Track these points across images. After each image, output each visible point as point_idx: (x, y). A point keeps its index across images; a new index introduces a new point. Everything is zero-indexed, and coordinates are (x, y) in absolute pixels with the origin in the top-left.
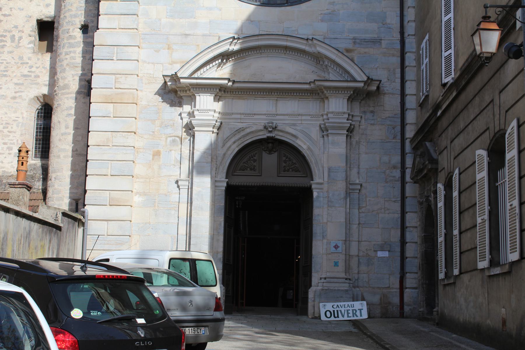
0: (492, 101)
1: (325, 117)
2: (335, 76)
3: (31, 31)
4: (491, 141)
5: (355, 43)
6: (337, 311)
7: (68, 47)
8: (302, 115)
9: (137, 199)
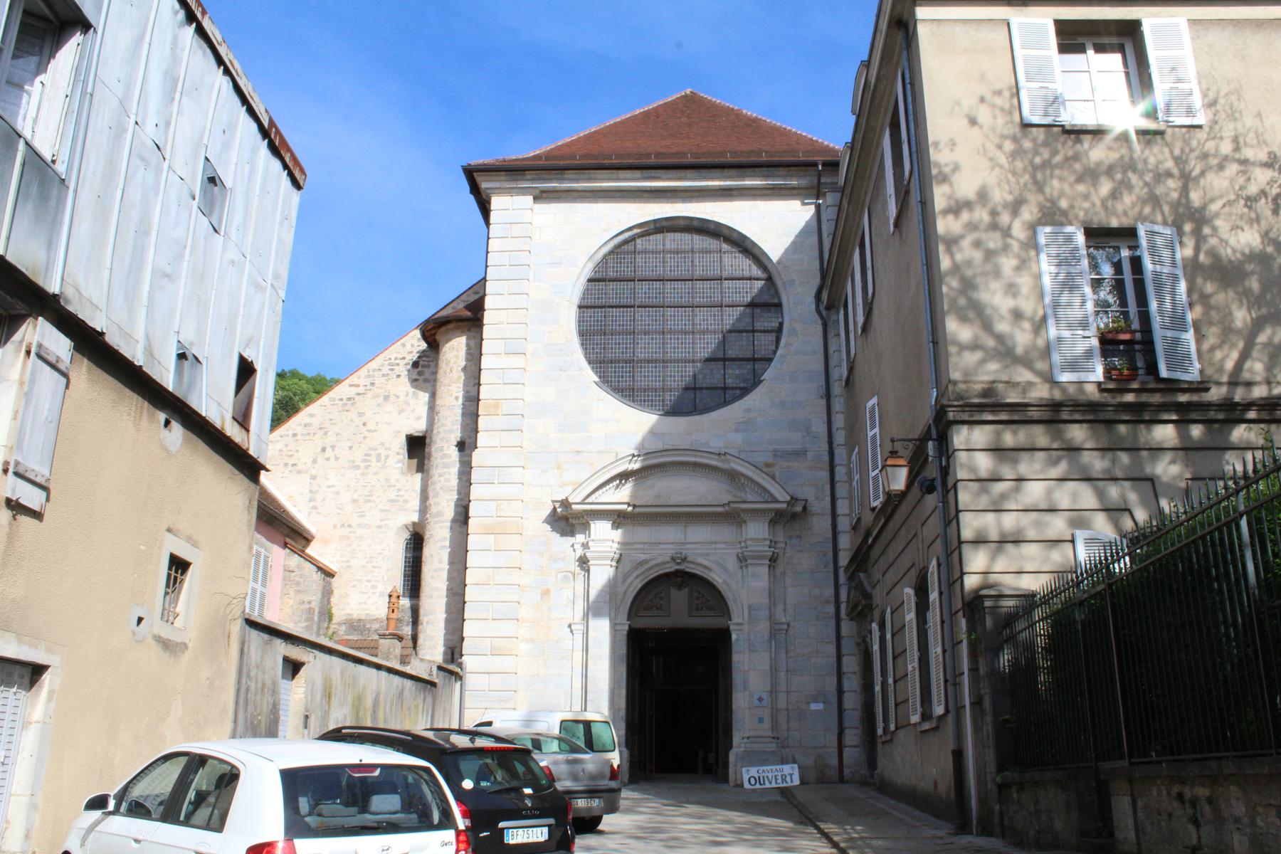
0: (916, 534)
1: (743, 544)
4: (917, 578)
5: (775, 456)
6: (763, 777)
8: (715, 543)
9: (523, 647)
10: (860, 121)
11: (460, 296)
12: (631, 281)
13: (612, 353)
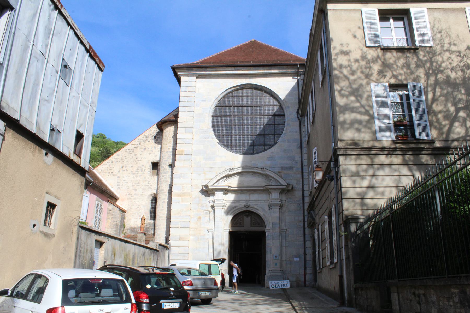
0: (328, 196)
1: (270, 201)
5: (282, 169)
6: (277, 285)
8: (260, 200)
9: (191, 238)
10: (310, 48)
12: (231, 107)
13: (224, 133)
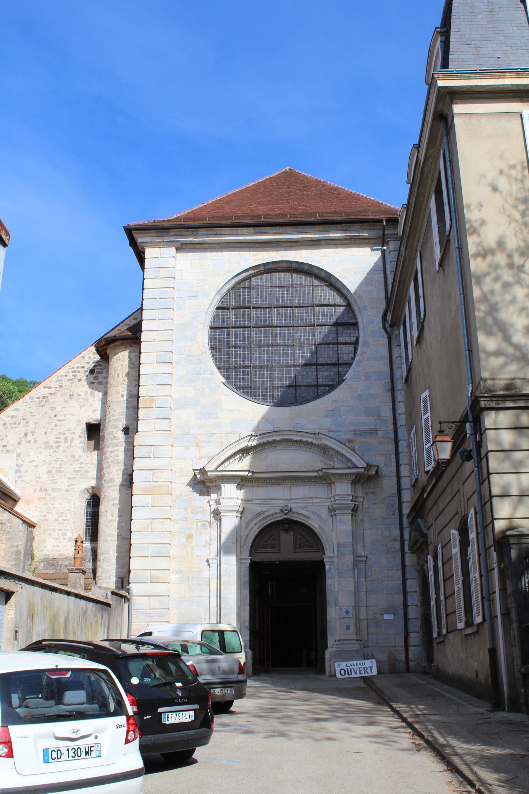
0: (459, 490)
1: (332, 499)
2: (339, 463)
3: (81, 433)
4: (460, 523)
5: (355, 434)
6: (351, 669)
7: (112, 446)
8: (312, 498)
9: (174, 577)
10: (413, 189)
11: (124, 321)
13: (235, 361)
